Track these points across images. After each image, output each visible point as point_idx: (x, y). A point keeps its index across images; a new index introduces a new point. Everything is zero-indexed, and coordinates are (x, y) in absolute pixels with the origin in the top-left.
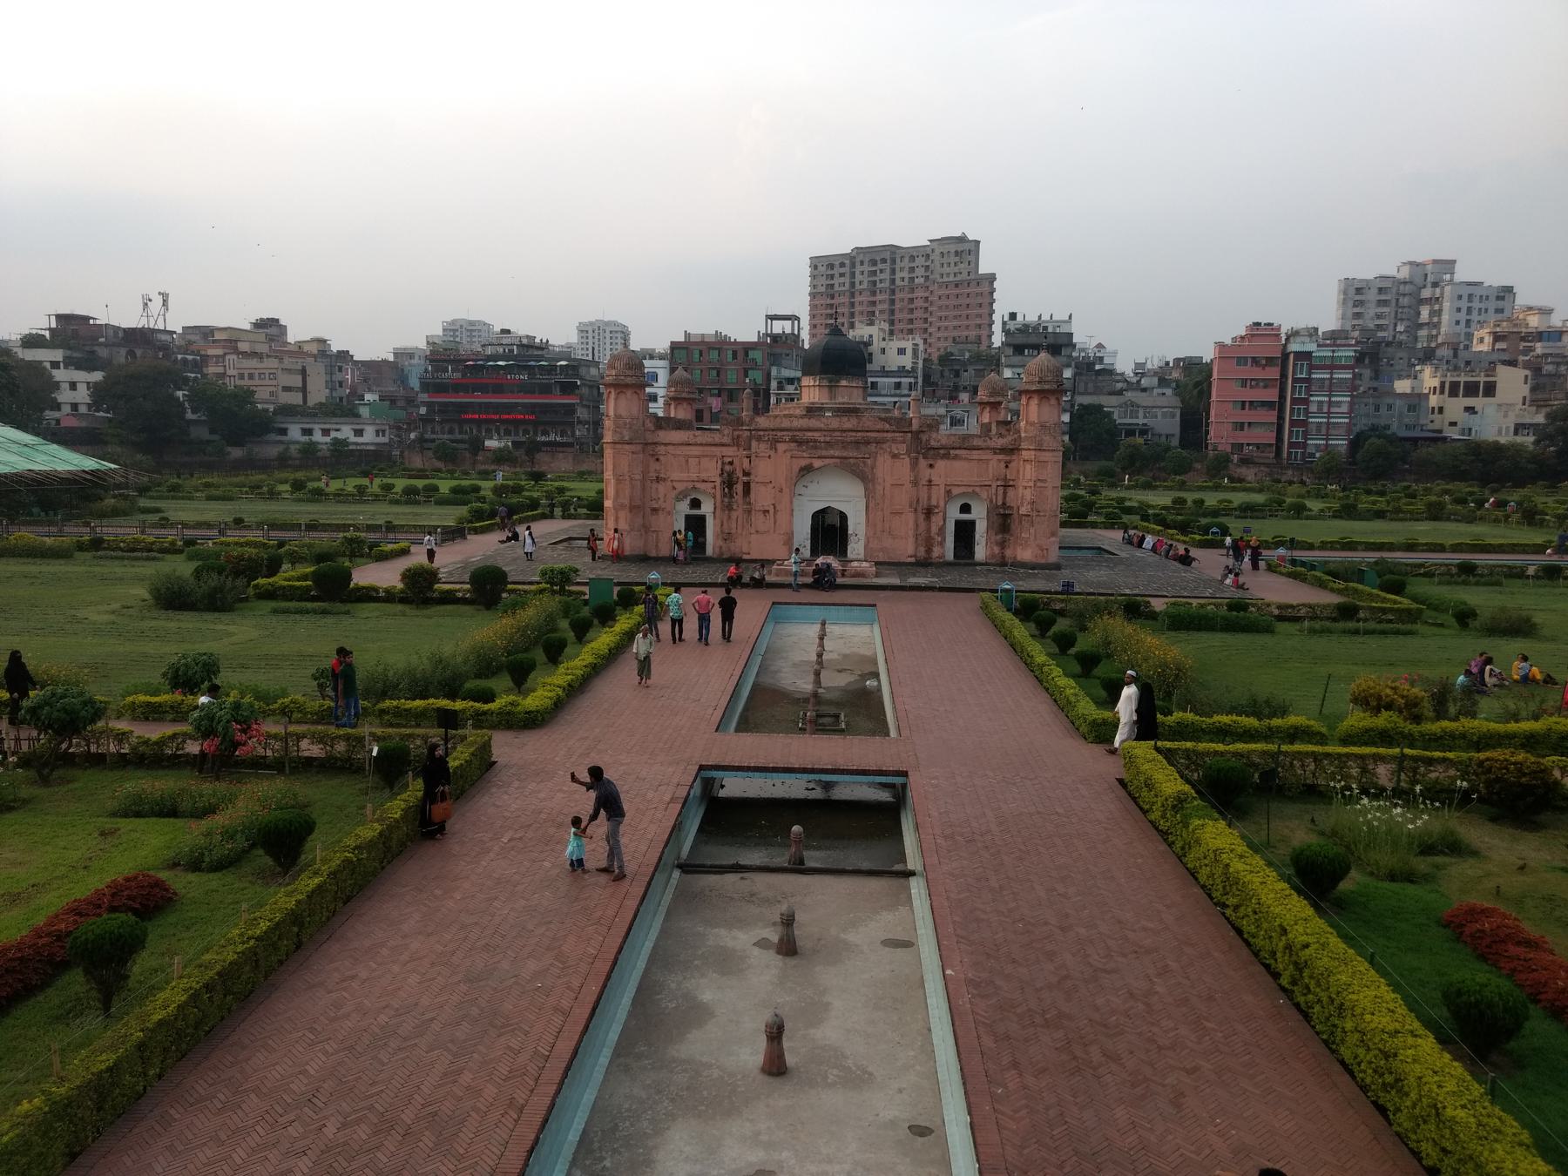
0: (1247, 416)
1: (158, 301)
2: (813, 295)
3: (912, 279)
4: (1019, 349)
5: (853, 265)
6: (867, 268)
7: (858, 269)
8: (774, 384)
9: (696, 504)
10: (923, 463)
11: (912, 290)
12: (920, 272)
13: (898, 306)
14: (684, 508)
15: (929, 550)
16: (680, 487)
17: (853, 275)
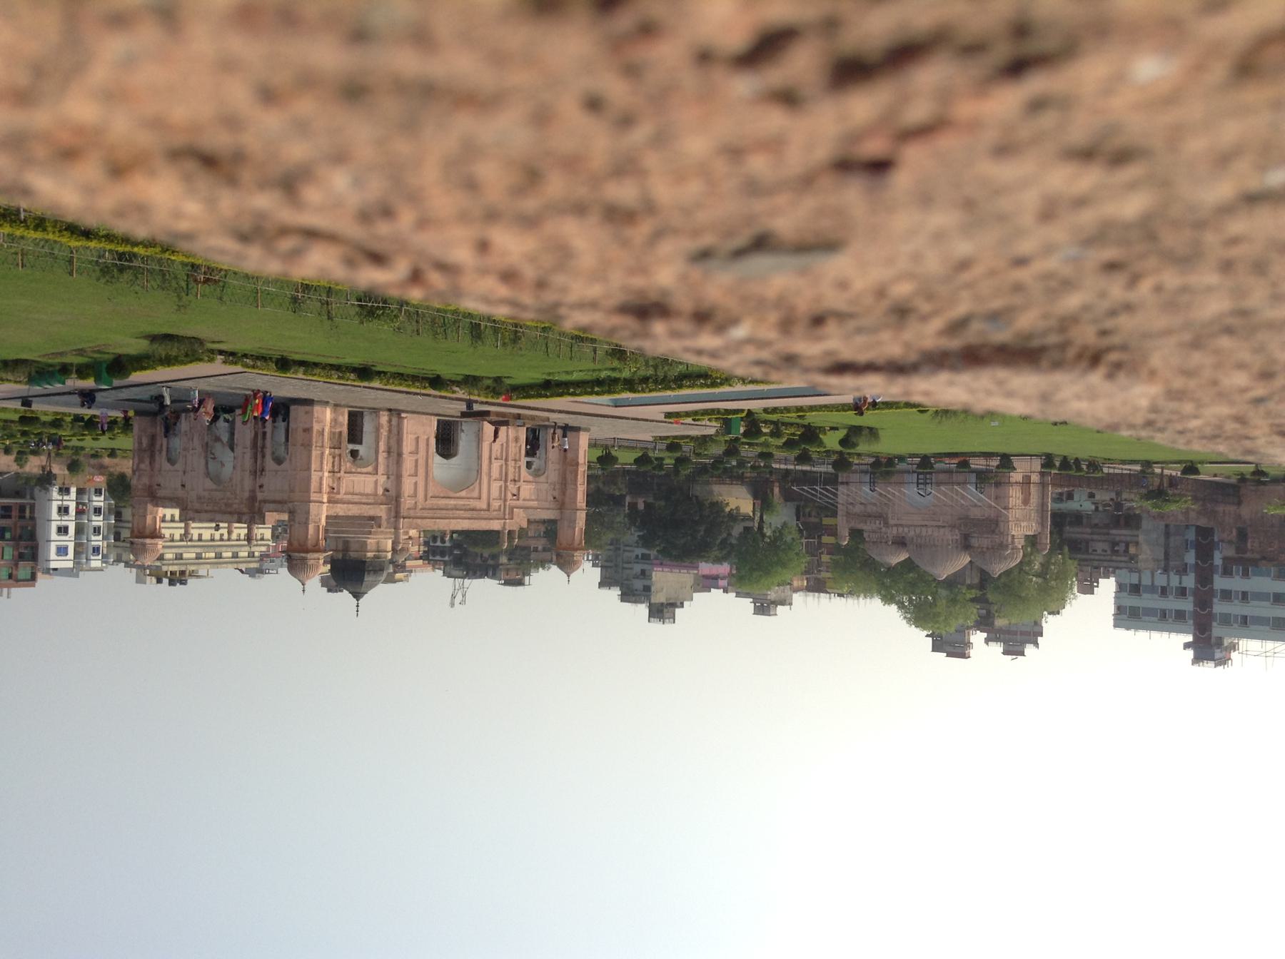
15: (390, 421)
16: (542, 479)
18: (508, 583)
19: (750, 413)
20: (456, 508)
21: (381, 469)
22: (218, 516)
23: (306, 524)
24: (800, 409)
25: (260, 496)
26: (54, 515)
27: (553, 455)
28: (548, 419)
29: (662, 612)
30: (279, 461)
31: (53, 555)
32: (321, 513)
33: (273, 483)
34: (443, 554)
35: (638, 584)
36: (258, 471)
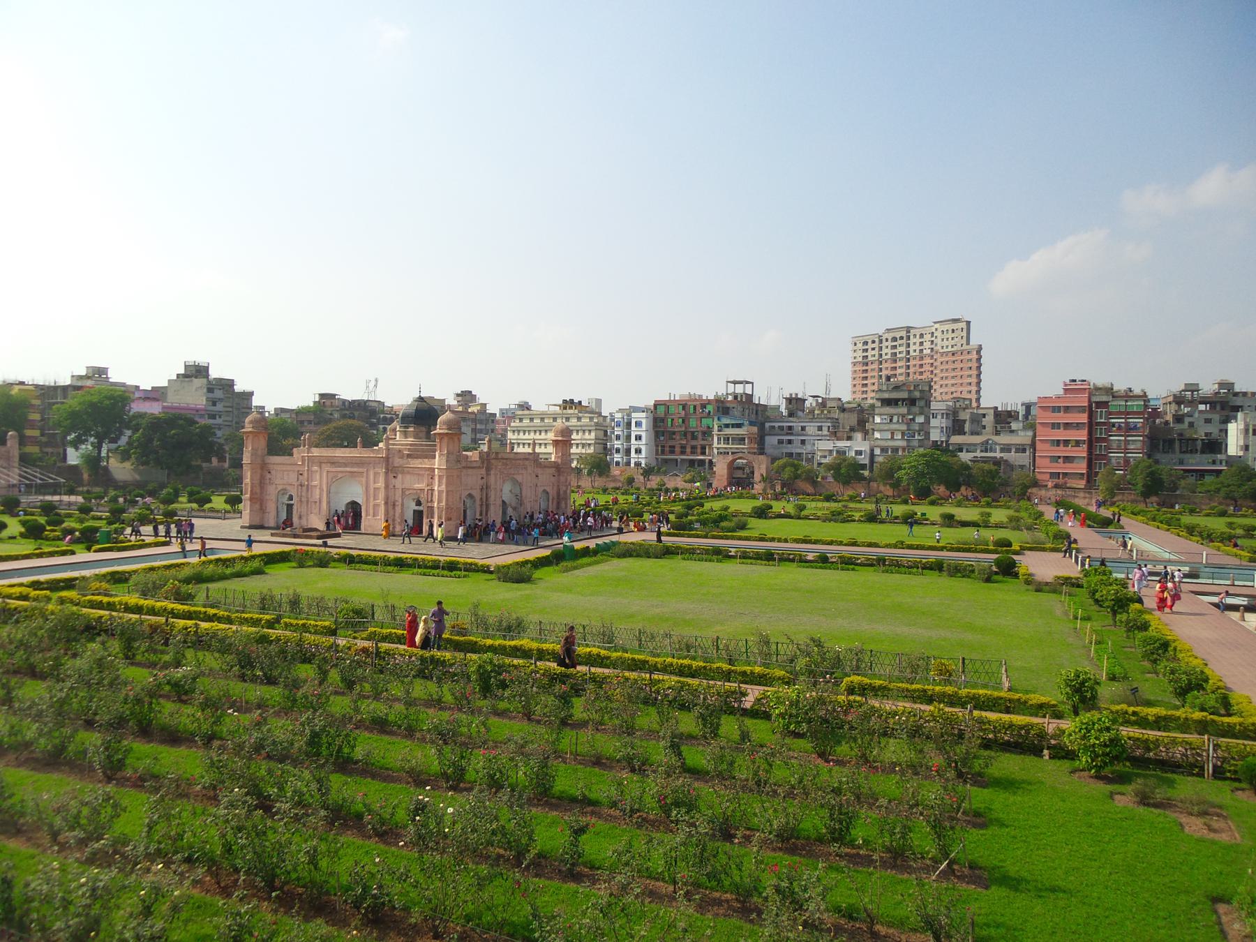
0: (1062, 451)
1: (373, 383)
2: (854, 364)
3: (921, 351)
4: (887, 402)
5: (881, 341)
6: (890, 344)
7: (885, 344)
8: (716, 427)
9: (291, 498)
10: (391, 475)
11: (922, 358)
12: (927, 345)
13: (911, 370)
14: (285, 500)
16: (280, 488)
17: (881, 349)
18: (333, 396)
19: (89, 549)
20: (346, 465)
21: (399, 493)
22: (512, 456)
23: (448, 453)
24: (40, 556)
25: (483, 471)
26: (643, 448)
27: (271, 507)
28: (272, 535)
29: (197, 372)
30: (470, 496)
31: (644, 421)
32: (438, 462)
33: (473, 481)
34: (385, 419)
35: (218, 394)
36: (485, 488)
